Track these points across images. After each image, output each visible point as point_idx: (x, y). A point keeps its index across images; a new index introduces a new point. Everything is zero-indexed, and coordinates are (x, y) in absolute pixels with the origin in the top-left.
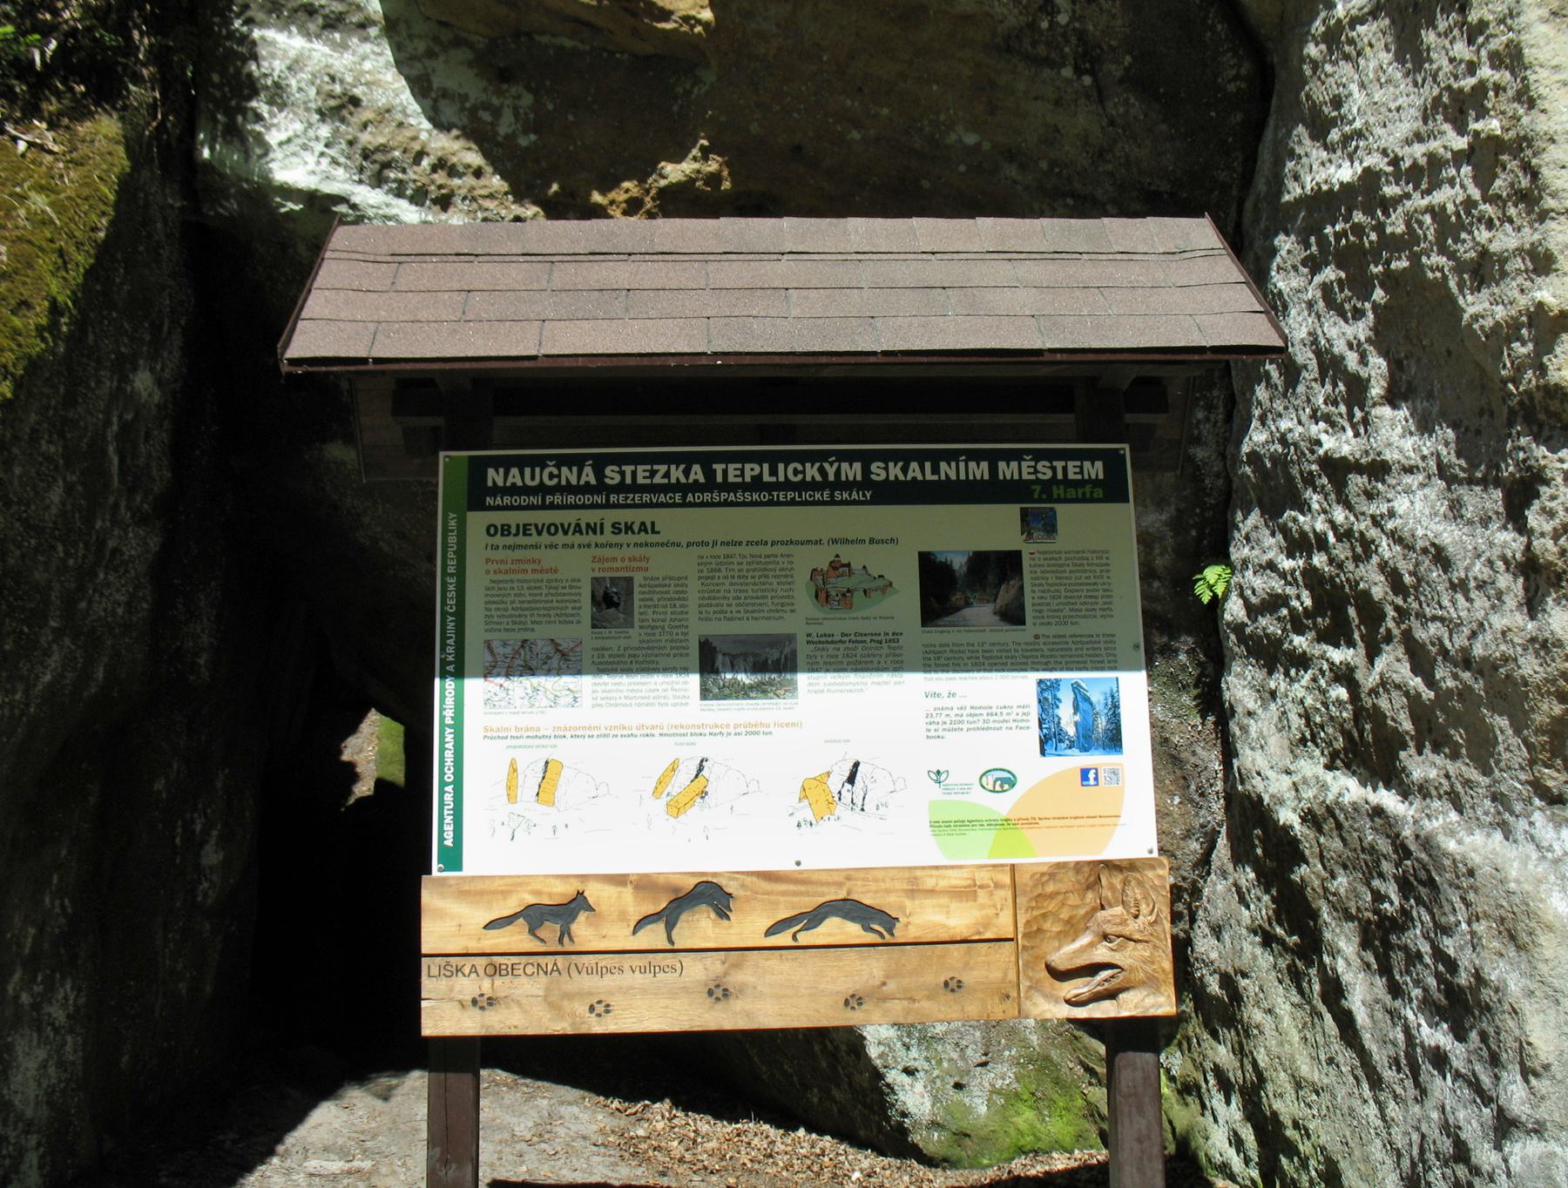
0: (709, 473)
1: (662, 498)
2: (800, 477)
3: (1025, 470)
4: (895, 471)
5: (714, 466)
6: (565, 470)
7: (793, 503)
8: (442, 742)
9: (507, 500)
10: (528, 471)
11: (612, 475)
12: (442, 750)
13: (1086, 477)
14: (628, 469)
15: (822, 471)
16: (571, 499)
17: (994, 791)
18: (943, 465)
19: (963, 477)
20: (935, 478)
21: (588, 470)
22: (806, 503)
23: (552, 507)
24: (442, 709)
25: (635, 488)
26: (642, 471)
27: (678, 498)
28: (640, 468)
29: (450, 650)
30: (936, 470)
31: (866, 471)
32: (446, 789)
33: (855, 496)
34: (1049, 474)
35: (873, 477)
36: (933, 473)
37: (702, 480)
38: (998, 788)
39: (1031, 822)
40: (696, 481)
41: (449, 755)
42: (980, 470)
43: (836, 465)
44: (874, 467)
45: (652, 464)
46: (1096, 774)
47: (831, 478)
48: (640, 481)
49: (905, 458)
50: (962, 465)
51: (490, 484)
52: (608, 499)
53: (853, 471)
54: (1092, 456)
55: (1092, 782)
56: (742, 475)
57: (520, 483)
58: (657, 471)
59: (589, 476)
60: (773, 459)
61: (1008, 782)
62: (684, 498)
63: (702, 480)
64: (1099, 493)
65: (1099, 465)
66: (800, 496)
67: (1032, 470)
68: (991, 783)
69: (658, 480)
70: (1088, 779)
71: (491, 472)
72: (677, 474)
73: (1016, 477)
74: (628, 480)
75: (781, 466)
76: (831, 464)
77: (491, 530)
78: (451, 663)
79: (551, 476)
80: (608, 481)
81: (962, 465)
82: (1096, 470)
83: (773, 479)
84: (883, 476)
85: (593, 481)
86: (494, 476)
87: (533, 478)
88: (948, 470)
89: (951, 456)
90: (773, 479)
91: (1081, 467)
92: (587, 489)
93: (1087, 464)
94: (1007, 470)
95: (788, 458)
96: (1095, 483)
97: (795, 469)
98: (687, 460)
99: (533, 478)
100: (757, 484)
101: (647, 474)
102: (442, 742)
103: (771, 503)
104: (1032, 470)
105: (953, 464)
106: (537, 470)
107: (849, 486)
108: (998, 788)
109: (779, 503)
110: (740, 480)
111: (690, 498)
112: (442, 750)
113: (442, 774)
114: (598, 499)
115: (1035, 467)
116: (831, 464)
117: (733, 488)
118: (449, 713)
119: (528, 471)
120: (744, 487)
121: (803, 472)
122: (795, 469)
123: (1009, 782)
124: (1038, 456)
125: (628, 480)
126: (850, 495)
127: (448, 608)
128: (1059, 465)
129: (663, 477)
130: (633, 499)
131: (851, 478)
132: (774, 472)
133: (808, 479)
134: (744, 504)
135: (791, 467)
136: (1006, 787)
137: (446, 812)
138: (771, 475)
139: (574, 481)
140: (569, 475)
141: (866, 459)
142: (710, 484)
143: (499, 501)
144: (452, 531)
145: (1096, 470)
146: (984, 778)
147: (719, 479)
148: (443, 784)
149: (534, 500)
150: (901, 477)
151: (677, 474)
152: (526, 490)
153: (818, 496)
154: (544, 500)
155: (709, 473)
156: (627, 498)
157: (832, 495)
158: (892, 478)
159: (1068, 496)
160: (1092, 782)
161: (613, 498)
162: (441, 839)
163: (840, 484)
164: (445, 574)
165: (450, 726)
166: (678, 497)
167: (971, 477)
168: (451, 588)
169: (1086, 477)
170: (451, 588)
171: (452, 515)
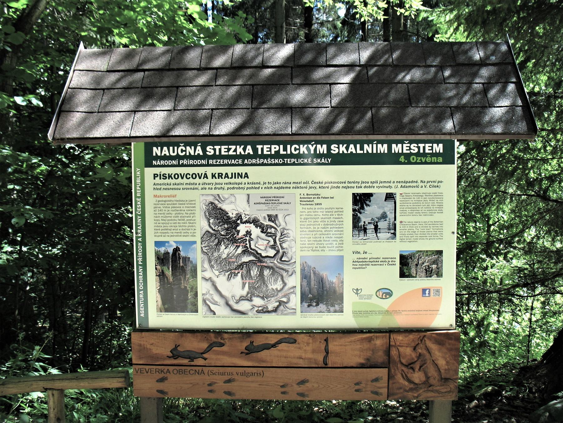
0: (255, 150)
2: (297, 152)
3: (405, 148)
4: (343, 149)
5: (257, 146)
6: (188, 148)
7: (294, 164)
9: (162, 162)
10: (171, 148)
11: (210, 150)
13: (434, 152)
15: (308, 149)
16: (191, 162)
18: (366, 146)
19: (375, 152)
20: (362, 152)
21: (199, 148)
23: (183, 165)
24: (137, 258)
25: (221, 157)
27: (240, 161)
28: (223, 147)
29: (139, 231)
30: (362, 148)
31: (329, 149)
34: (416, 150)
35: (332, 152)
38: (384, 297)
40: (249, 153)
42: (383, 148)
43: (315, 146)
44: (332, 147)
46: (429, 291)
47: (312, 152)
48: (223, 153)
50: (375, 146)
51: (154, 154)
52: (208, 162)
53: (322, 149)
54: (438, 142)
55: (427, 295)
56: (270, 151)
57: (168, 154)
59: (199, 151)
62: (243, 161)
63: (252, 153)
64: (440, 159)
65: (441, 145)
66: (297, 161)
67: (408, 148)
69: (231, 153)
71: (155, 149)
72: (240, 150)
73: (400, 152)
74: (217, 153)
75: (289, 146)
76: (312, 145)
77: (155, 176)
78: (140, 237)
79: (182, 151)
80: (208, 153)
81: (375, 146)
82: (438, 148)
83: (285, 153)
84: (337, 151)
85: (201, 154)
86: (156, 151)
87: (174, 152)
89: (369, 142)
90: (285, 153)
91: (432, 147)
92: (198, 157)
93: (435, 145)
94: (396, 148)
96: (437, 155)
97: (295, 148)
99: (174, 152)
100: (277, 155)
101: (226, 150)
103: (284, 164)
104: (408, 148)
105: (370, 145)
106: (176, 148)
107: (320, 156)
108: (384, 297)
109: (287, 164)
110: (269, 153)
111: (246, 161)
112: (138, 275)
114: (203, 162)
115: (410, 147)
116: (312, 145)
117: (266, 157)
118: (140, 259)
119: (171, 148)
121: (299, 149)
122: (295, 148)
123: (388, 294)
125: (217, 153)
126: (321, 161)
128: (421, 146)
130: (220, 162)
131: (322, 152)
132: (285, 149)
134: (271, 165)
138: (284, 151)
139: (192, 154)
140: (190, 150)
142: (255, 155)
143: (158, 163)
144: (138, 177)
145: (438, 148)
147: (260, 153)
149: (174, 162)
150: (345, 152)
151: (240, 150)
152: (170, 158)
154: (179, 162)
155: (255, 150)
156: (217, 162)
158: (341, 152)
160: (427, 295)
161: (211, 162)
162: (139, 314)
164: (136, 197)
165: (140, 265)
167: (379, 152)
168: (139, 203)
170: (139, 203)
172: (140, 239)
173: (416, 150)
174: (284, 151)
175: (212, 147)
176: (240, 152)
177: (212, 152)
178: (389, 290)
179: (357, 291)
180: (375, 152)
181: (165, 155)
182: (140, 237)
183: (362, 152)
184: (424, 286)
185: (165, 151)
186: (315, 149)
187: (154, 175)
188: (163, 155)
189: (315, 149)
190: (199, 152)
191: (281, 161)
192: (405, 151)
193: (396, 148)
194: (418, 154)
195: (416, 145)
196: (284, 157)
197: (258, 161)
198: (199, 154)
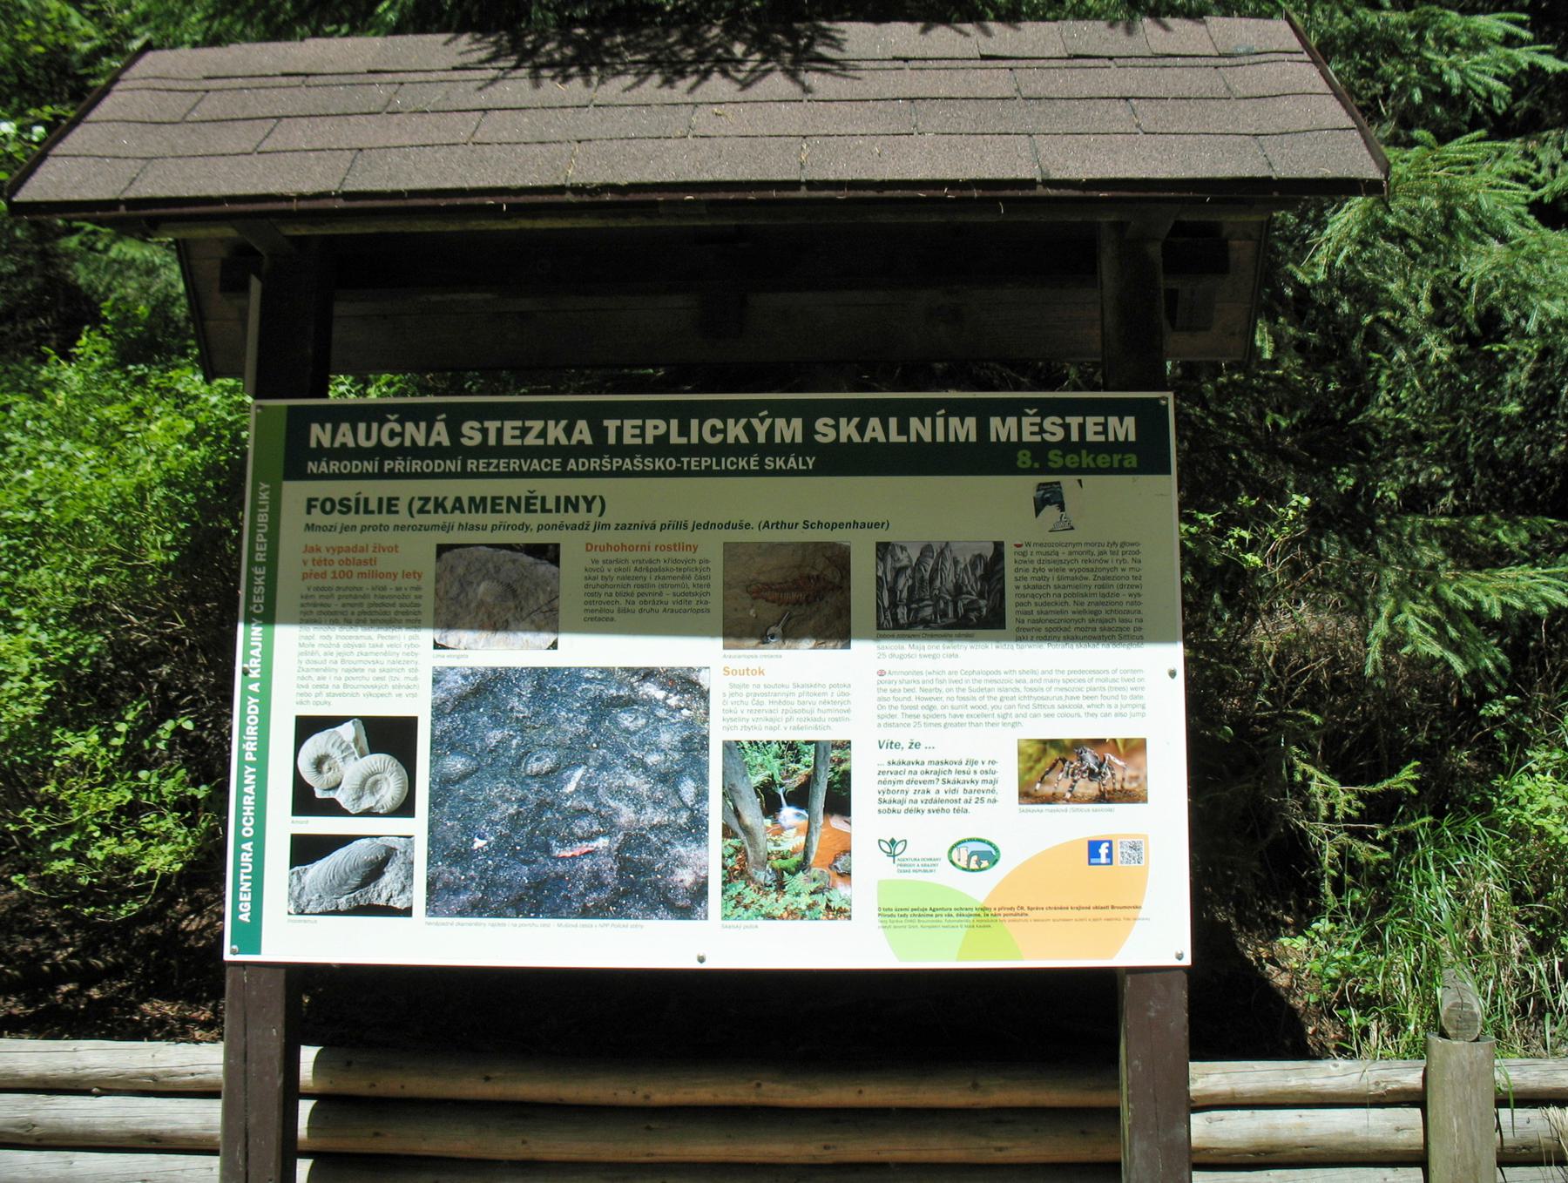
0: (598, 432)
1: (535, 465)
2: (720, 437)
4: (848, 430)
5: (606, 423)
6: (410, 426)
7: (708, 472)
8: (241, 785)
9: (335, 466)
11: (471, 433)
12: (240, 794)
13: (1111, 438)
14: (492, 426)
16: (416, 465)
18: (914, 422)
19: (940, 438)
20: (903, 439)
21: (440, 427)
22: (726, 473)
23: (393, 475)
24: (242, 742)
25: (501, 451)
27: (556, 464)
28: (508, 425)
30: (903, 429)
31: (809, 430)
32: (244, 846)
33: (792, 463)
34: (1060, 434)
35: (818, 438)
36: (900, 433)
37: (588, 441)
38: (973, 865)
39: (1017, 913)
40: (581, 442)
41: (248, 801)
42: (964, 429)
43: (768, 422)
44: (819, 424)
45: (524, 418)
46: (1110, 848)
47: (761, 439)
48: (507, 441)
49: (863, 412)
50: (940, 422)
51: (313, 444)
52: (464, 465)
53: (790, 430)
54: (1120, 409)
55: (1103, 859)
56: (642, 435)
57: (351, 444)
58: (530, 429)
59: (441, 434)
60: (684, 413)
61: (989, 857)
62: (564, 465)
63: (588, 441)
64: (1132, 460)
65: (1130, 421)
66: (719, 463)
67: (1036, 429)
69: (530, 440)
70: (1099, 856)
71: (315, 429)
72: (556, 432)
73: (1014, 438)
74: (492, 441)
75: (694, 423)
76: (762, 420)
79: (392, 434)
80: (465, 441)
81: (940, 422)
83: (684, 440)
85: (446, 442)
86: (319, 434)
87: (368, 437)
88: (920, 429)
89: (926, 410)
90: (684, 440)
91: (1105, 425)
92: (437, 452)
93: (1113, 421)
94: (1002, 429)
95: (704, 411)
97: (713, 427)
98: (569, 414)
99: (368, 437)
100: (662, 446)
101: (517, 433)
102: (241, 785)
103: (679, 473)
105: (928, 420)
106: (375, 426)
107: (785, 450)
109: (689, 473)
110: (638, 441)
111: (572, 465)
112: (240, 794)
113: (239, 826)
114: (451, 465)
115: (1040, 425)
116: (762, 420)
118: (250, 747)
119: (362, 427)
121: (724, 431)
122: (713, 427)
123: (989, 857)
124: (1046, 409)
125: (492, 441)
126: (786, 462)
128: (1074, 421)
129: (538, 437)
130: (497, 466)
132: (684, 431)
133: (731, 440)
135: (708, 424)
136: (985, 864)
137: (243, 877)
139: (421, 442)
140: (415, 433)
141: (810, 413)
142: (600, 447)
143: (324, 468)
144: (263, 506)
145: (1125, 428)
147: (612, 440)
148: (240, 839)
149: (368, 466)
150: (856, 438)
151: (556, 432)
152: (359, 453)
153: (742, 463)
155: (598, 432)
156: (489, 464)
157: (761, 463)
158: (843, 439)
160: (1103, 859)
161: (471, 465)
163: (772, 448)
164: (252, 563)
165: (251, 764)
166: (556, 463)
167: (952, 439)
168: (259, 581)
170: (259, 581)
171: (264, 486)
172: (254, 687)
173: (1060, 434)
176: (557, 440)
178: (990, 844)
179: (892, 847)
180: (940, 438)
181: (344, 445)
183: (903, 439)
184: (1095, 835)
185: (345, 436)
186: (770, 432)
187: (310, 500)
188: (337, 444)
189: (770, 432)
191: (671, 463)
192: (1027, 438)
193: (1002, 429)
194: (1066, 446)
195: (1058, 420)
196: (679, 452)
197: (607, 464)
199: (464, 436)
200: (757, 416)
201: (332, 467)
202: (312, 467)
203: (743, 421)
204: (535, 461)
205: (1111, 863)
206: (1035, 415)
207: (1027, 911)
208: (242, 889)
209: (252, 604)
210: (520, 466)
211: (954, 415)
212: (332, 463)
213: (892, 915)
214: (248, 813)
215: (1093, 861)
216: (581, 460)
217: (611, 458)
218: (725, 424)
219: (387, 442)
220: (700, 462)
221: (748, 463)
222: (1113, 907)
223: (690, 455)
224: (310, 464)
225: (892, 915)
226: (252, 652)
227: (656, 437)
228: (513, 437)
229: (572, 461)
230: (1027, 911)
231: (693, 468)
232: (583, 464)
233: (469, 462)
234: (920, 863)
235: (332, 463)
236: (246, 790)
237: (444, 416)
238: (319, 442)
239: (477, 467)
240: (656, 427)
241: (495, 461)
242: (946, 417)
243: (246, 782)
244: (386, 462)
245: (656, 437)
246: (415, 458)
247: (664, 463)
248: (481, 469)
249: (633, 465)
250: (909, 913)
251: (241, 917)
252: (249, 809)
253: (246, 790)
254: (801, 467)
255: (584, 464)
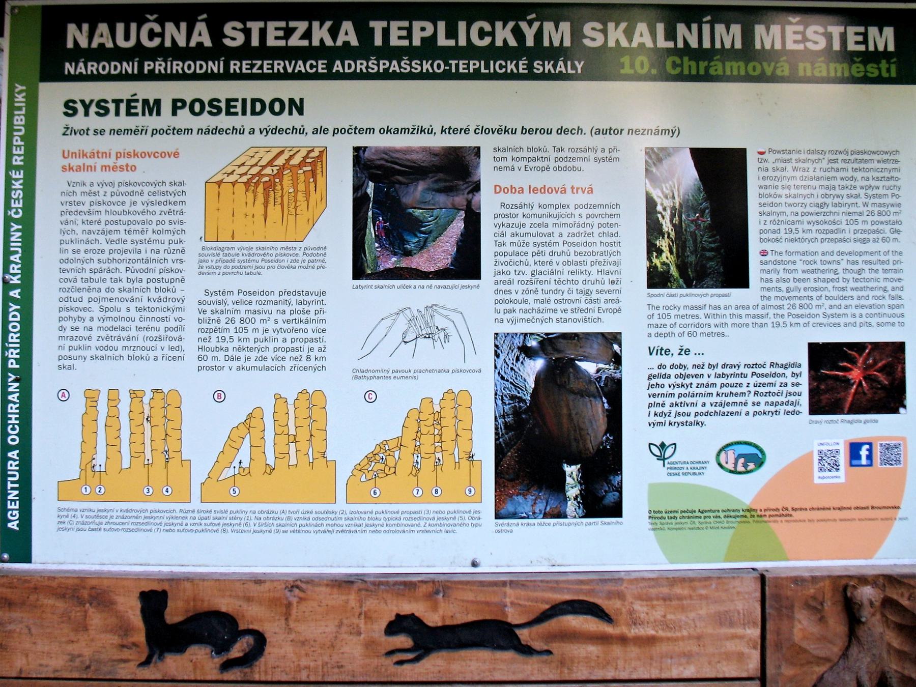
0: (365, 34)
1: (300, 67)
2: (487, 40)
3: (790, 37)
5: (372, 24)
6: (170, 27)
7: (476, 75)
9: (92, 67)
10: (120, 27)
11: (233, 34)
13: (871, 48)
14: (255, 26)
15: (518, 33)
16: (177, 66)
17: (734, 472)
18: (681, 28)
19: (707, 44)
21: (201, 27)
23: (153, 76)
25: (265, 52)
26: (273, 29)
28: (271, 25)
38: (740, 468)
39: (784, 513)
40: (346, 44)
43: (536, 25)
47: (530, 42)
48: (271, 42)
50: (706, 28)
51: (70, 45)
52: (227, 66)
55: (864, 461)
56: (409, 37)
57: (110, 45)
58: (294, 29)
59: (202, 35)
62: (330, 66)
63: (354, 42)
65: (889, 32)
66: (487, 66)
67: (799, 37)
68: (731, 460)
69: (295, 41)
71: (72, 28)
72: (321, 34)
74: (255, 42)
75: (462, 25)
76: (530, 23)
77: (70, 108)
78: (15, 287)
79: (152, 35)
80: (227, 42)
81: (706, 28)
83: (452, 43)
84: (599, 43)
85: (208, 43)
86: (76, 35)
87: (127, 38)
90: (452, 43)
91: (865, 35)
92: (199, 53)
93: (873, 31)
99: (127, 38)
100: (429, 49)
103: (447, 75)
104: (799, 37)
105: (694, 27)
106: (133, 26)
109: (458, 76)
110: (405, 43)
111: (338, 66)
114: (214, 67)
115: (803, 33)
116: (530, 23)
119: (120, 27)
120: (411, 53)
121: (492, 34)
125: (255, 42)
126: (555, 66)
127: (12, 213)
129: (302, 38)
130: (261, 67)
132: (452, 33)
133: (499, 43)
136: (751, 466)
138: (448, 37)
139: (182, 43)
142: (366, 49)
143: (81, 69)
144: (20, 109)
146: (723, 454)
147: (378, 41)
149: (128, 67)
151: (321, 34)
152: (119, 54)
153: (511, 67)
154: (141, 67)
155: (365, 34)
157: (530, 67)
159: (817, 74)
160: (864, 461)
161: (234, 66)
167: (718, 45)
168: (17, 185)
169: (871, 48)
170: (17, 185)
171: (20, 88)
172: (16, 293)
174: (448, 37)
175: (239, 25)
176: (322, 41)
177: (240, 39)
178: (756, 447)
179: (662, 451)
180: (707, 44)
182: (15, 287)
185: (103, 36)
186: (539, 36)
189: (539, 36)
190: (200, 39)
191: (439, 66)
192: (790, 46)
197: (373, 66)
198: (200, 44)
199: (226, 37)
200: (524, 19)
201: (89, 68)
202: (69, 68)
203: (511, 24)
204: (300, 62)
205: (871, 465)
206: (797, 23)
207: (791, 512)
208: (10, 497)
209: (11, 209)
210: (285, 68)
211: (720, 22)
212: (90, 64)
213: (662, 518)
214: (13, 421)
215: (855, 462)
216: (346, 62)
217: (378, 60)
218: (493, 27)
219: (146, 43)
220: (468, 65)
221: (517, 66)
222: (873, 507)
223: (459, 58)
224: (67, 65)
225: (662, 518)
226: (12, 258)
227: (423, 39)
228: (277, 38)
229: (338, 62)
230: (791, 512)
231: (461, 71)
232: (350, 66)
233: (232, 63)
234: (689, 466)
235: (90, 64)
236: (10, 397)
237: (205, 16)
238: (76, 42)
239: (241, 68)
240: (423, 29)
241: (259, 63)
242: (712, 24)
243: (10, 389)
244: (146, 63)
245: (423, 39)
246: (175, 59)
247: (432, 65)
248: (244, 71)
249: (400, 67)
250: (678, 515)
251: (10, 525)
252: (13, 416)
253: (10, 397)
254: (570, 71)
255: (350, 66)
